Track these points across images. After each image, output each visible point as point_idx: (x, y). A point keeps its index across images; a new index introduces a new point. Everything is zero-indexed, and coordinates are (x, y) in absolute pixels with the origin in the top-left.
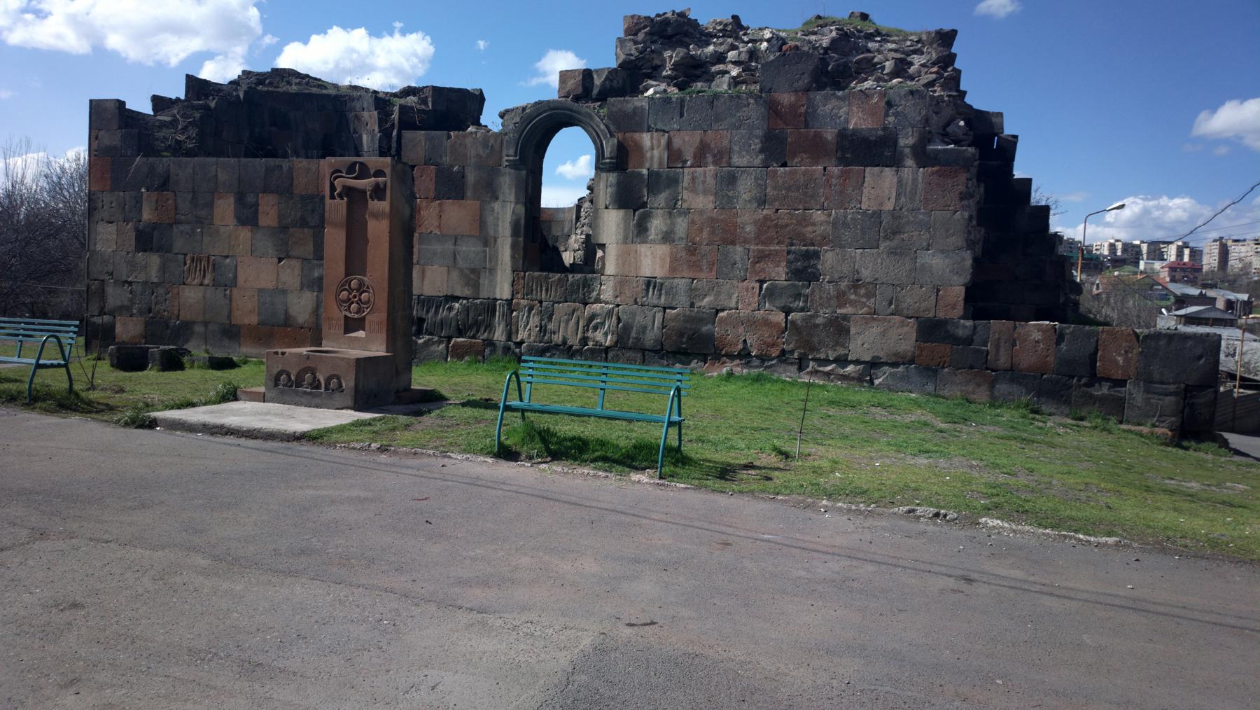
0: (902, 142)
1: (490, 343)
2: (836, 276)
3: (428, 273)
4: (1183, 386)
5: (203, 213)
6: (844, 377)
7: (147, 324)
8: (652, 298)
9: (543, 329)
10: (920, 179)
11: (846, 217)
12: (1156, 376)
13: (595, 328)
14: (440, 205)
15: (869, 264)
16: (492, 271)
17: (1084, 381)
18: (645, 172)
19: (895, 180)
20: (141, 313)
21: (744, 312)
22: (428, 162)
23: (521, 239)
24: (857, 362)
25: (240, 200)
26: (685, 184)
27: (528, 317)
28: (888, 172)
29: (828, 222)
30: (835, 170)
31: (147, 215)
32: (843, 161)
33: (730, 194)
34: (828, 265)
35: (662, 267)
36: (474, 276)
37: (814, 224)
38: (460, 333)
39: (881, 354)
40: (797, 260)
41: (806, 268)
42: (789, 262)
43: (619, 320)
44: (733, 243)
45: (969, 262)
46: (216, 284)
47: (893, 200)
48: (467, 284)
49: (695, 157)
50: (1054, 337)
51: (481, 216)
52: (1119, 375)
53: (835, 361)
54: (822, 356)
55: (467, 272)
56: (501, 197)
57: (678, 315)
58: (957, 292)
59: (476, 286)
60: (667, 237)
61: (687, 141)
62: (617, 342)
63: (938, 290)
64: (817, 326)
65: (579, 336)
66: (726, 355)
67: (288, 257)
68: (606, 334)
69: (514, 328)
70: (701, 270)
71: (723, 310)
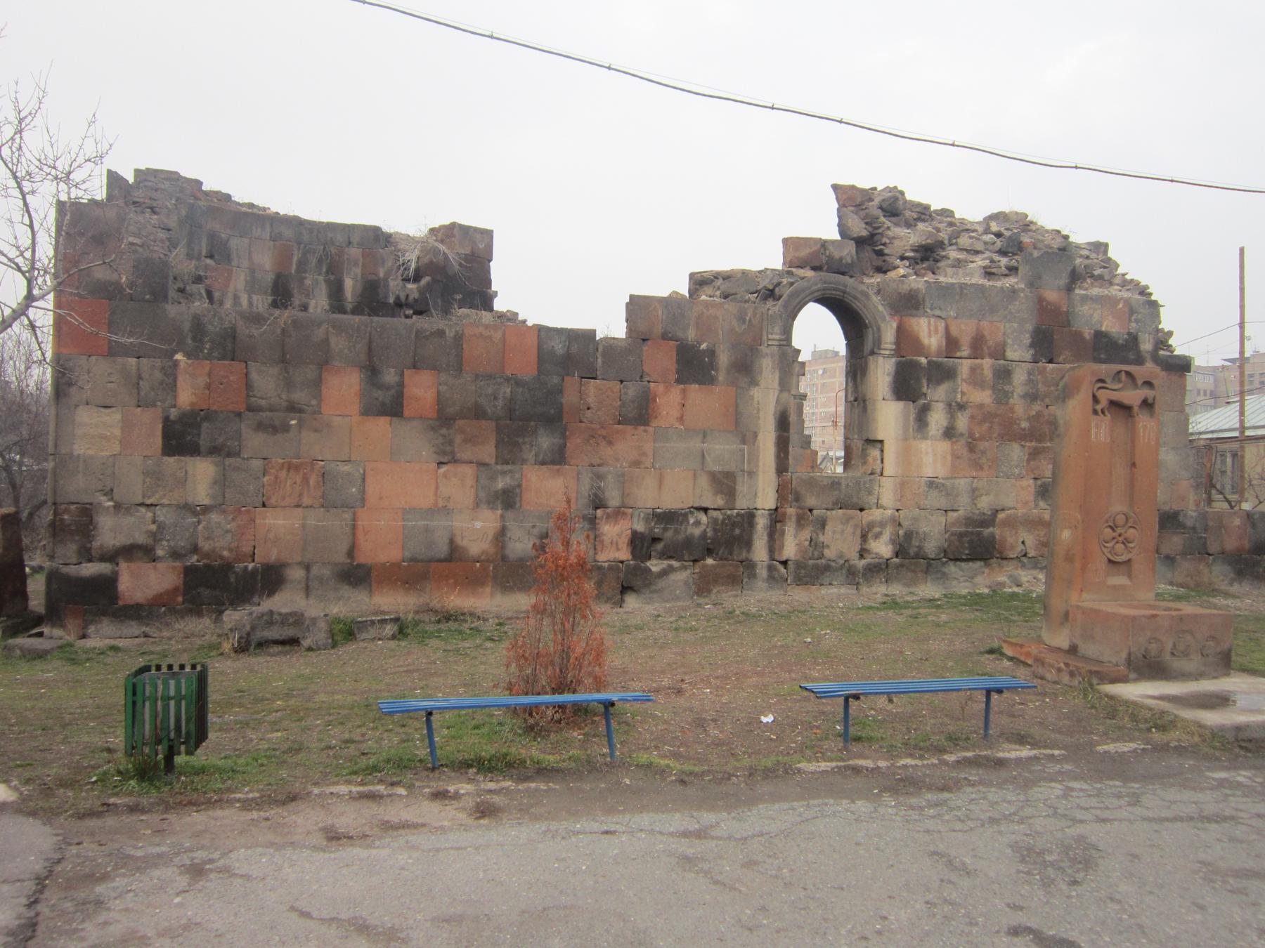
5: (299, 396)
7: (189, 571)
8: (936, 500)
14: (684, 391)
16: (751, 474)
18: (923, 360)
20: (175, 555)
21: (1021, 511)
22: (665, 337)
25: (372, 372)
31: (186, 396)
33: (1006, 388)
38: (709, 552)
46: (327, 505)
51: (737, 406)
56: (763, 382)
59: (731, 494)
60: (949, 433)
61: (965, 330)
65: (858, 548)
67: (455, 461)
70: (982, 468)
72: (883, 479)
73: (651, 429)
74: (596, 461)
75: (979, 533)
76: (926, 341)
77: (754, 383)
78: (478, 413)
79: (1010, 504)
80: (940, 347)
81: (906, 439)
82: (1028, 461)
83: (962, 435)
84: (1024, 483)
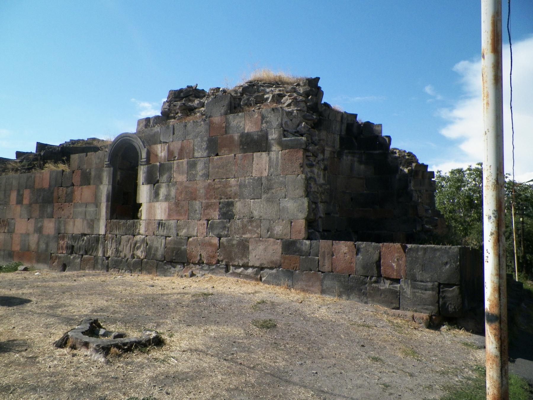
0: (270, 137)
1: (96, 258)
2: (242, 216)
3: (76, 223)
4: (436, 283)
6: (247, 277)
8: (161, 232)
9: (117, 251)
10: (280, 158)
11: (245, 182)
12: (419, 277)
13: (138, 249)
15: (258, 208)
16: (99, 220)
17: (374, 279)
19: (268, 159)
21: (200, 238)
23: (110, 203)
24: (253, 267)
25: (19, 191)
26: (175, 169)
27: (112, 243)
28: (264, 154)
29: (237, 185)
30: (239, 155)
32: (244, 151)
33: (194, 172)
34: (237, 210)
35: (165, 214)
36: (92, 223)
37: (231, 187)
39: (265, 262)
40: (223, 207)
41: (228, 211)
42: (220, 209)
43: (147, 244)
44: (195, 199)
45: (306, 204)
47: (267, 170)
48: (89, 227)
49: (179, 155)
50: (355, 251)
52: (394, 276)
53: (243, 266)
54: (236, 264)
55: (89, 221)
57: (171, 240)
58: (301, 224)
60: (167, 198)
62: (146, 256)
63: (291, 223)
64: (233, 245)
66: (192, 263)
68: (142, 252)
69: (106, 251)
71: (191, 237)
72: (141, 221)
73: (73, 204)
74: (59, 217)
75: (179, 249)
76: (160, 155)
77: (101, 183)
78: (36, 202)
79: (195, 234)
80: (165, 156)
81: (150, 202)
82: (204, 210)
83: (173, 198)
84: (201, 222)
